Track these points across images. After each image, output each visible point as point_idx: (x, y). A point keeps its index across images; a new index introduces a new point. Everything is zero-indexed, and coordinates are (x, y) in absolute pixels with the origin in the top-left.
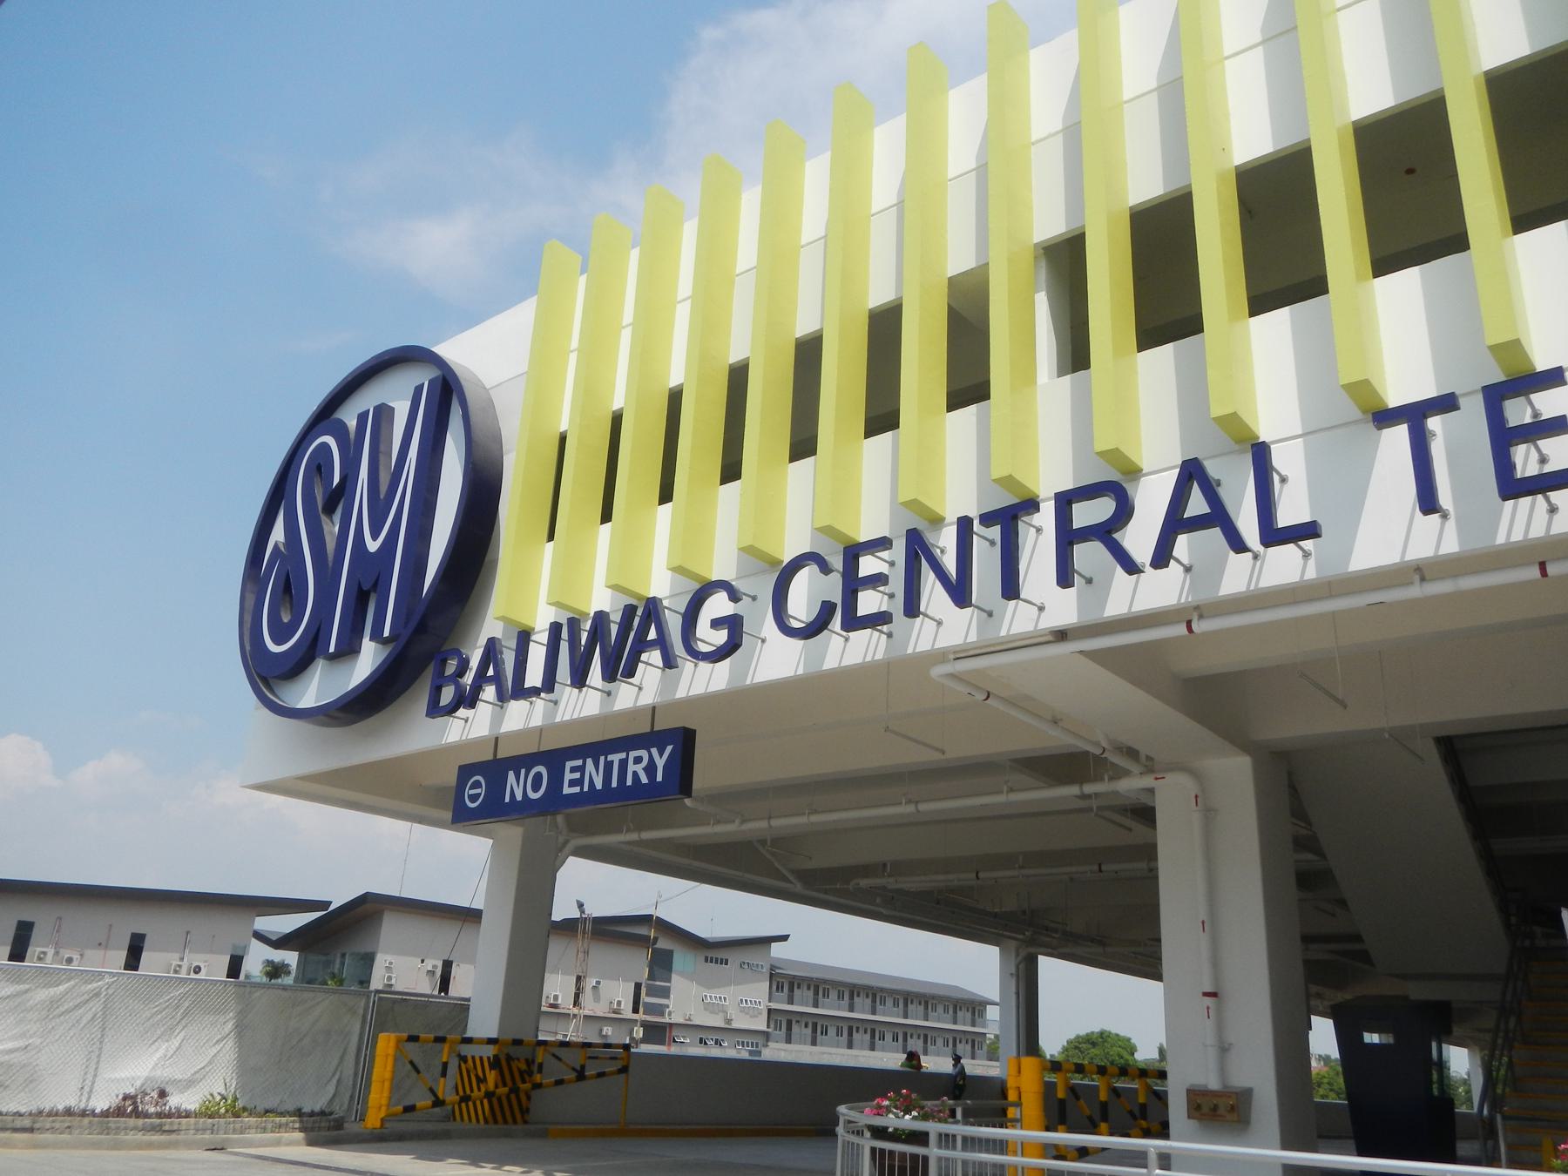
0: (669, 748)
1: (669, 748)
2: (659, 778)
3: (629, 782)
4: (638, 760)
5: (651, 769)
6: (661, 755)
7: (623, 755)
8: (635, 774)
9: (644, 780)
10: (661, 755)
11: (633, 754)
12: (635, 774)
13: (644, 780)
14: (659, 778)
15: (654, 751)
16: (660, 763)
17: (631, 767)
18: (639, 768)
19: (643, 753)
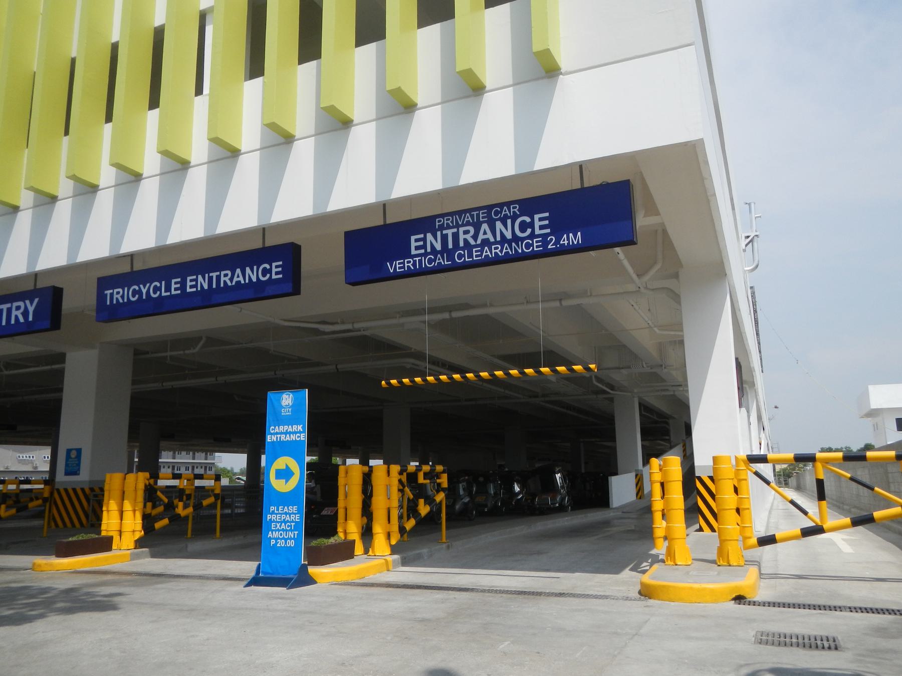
0: (36, 300)
1: (36, 300)
2: (31, 319)
3: (13, 322)
4: (18, 308)
5: (25, 314)
6: (31, 304)
7: (9, 305)
8: (16, 317)
9: (22, 320)
10: (31, 304)
11: (15, 304)
12: (16, 317)
13: (22, 320)
14: (31, 319)
15: (28, 302)
16: (31, 309)
17: (14, 313)
18: (19, 313)
19: (21, 304)
